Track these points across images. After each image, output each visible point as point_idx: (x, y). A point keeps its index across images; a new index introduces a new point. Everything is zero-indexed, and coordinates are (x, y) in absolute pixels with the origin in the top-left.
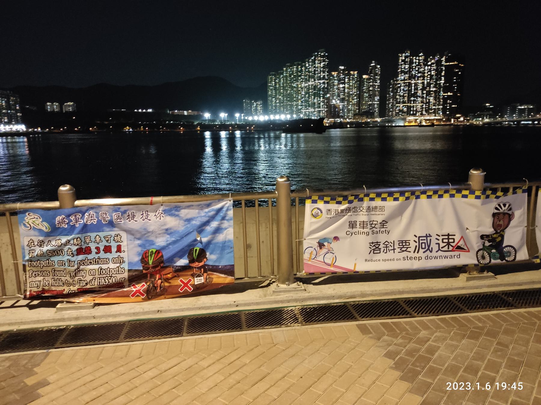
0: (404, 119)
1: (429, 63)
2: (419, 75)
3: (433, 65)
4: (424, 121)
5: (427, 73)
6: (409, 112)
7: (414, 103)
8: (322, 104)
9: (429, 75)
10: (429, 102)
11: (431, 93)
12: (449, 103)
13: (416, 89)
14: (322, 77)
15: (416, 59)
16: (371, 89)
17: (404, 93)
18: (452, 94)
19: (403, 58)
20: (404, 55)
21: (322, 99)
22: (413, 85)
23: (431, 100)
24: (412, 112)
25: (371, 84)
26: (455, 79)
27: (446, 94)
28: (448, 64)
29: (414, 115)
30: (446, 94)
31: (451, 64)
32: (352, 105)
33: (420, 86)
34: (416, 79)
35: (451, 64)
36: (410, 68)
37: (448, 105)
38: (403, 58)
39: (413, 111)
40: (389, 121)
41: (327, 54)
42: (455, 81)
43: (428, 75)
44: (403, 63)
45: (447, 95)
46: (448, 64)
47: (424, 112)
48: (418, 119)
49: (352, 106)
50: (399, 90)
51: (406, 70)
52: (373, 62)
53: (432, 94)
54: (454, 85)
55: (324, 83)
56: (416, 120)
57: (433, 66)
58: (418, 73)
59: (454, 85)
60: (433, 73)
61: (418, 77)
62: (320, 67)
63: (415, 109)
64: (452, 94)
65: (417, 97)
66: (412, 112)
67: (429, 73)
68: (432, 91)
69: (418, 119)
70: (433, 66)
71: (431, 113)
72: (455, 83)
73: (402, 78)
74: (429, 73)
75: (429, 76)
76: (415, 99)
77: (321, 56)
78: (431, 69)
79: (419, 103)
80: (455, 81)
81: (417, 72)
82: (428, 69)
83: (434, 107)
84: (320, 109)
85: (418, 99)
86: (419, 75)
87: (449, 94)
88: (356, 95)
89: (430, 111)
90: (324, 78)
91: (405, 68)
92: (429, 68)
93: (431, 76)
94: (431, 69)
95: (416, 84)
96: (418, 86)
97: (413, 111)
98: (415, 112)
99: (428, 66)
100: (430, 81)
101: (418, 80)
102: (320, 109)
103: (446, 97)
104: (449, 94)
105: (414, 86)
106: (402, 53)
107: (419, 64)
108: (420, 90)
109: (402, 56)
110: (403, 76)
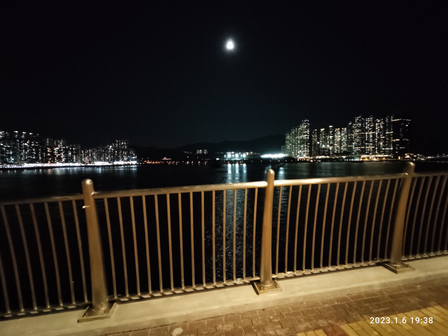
0: (359, 157)
1: (379, 121)
2: (370, 129)
3: (381, 122)
4: (375, 158)
5: (377, 127)
6: (363, 152)
7: (368, 146)
8: (305, 148)
9: (379, 128)
10: (380, 145)
11: (381, 140)
12: (398, 146)
13: (369, 138)
14: (305, 133)
15: (368, 119)
16: (349, 138)
17: (359, 141)
18: (399, 140)
19: (358, 120)
20: (358, 117)
21: (305, 146)
22: (367, 135)
23: (381, 145)
24: (367, 152)
25: (349, 135)
26: (401, 130)
27: (395, 140)
28: (395, 120)
29: (368, 154)
30: (395, 140)
31: (397, 120)
32: (343, 147)
33: (371, 136)
34: (368, 131)
35: (397, 120)
36: (362, 125)
37: (397, 147)
38: (358, 120)
39: (367, 151)
40: (351, 158)
41: (308, 121)
42: (401, 131)
43: (378, 129)
44: (358, 122)
45: (396, 141)
46: (395, 120)
47: (377, 152)
48: (370, 157)
49: (343, 148)
50: (356, 138)
51: (360, 127)
52: (351, 122)
53: (382, 140)
54: (400, 134)
55: (307, 137)
56: (369, 157)
57: (382, 123)
58: (369, 128)
59: (400, 134)
60: (382, 127)
61: (370, 130)
62: (305, 128)
63: (368, 150)
64: (399, 140)
65: (369, 142)
66: (367, 152)
67: (379, 127)
68: (382, 139)
69: (370, 157)
70: (382, 123)
71: (382, 153)
72: (401, 132)
73: (358, 131)
74: (379, 127)
75: (379, 129)
76: (368, 144)
77: (305, 122)
78: (380, 124)
79: (371, 146)
80: (401, 131)
81: (369, 127)
82: (378, 125)
83: (383, 149)
84: (304, 151)
85: (370, 144)
86: (370, 129)
87: (397, 140)
88: (345, 142)
89: (381, 152)
90: (307, 134)
91: (359, 126)
92: (379, 124)
93: (380, 129)
94: (380, 124)
95: (368, 135)
96: (370, 136)
97: (367, 151)
98: (368, 152)
99: (378, 123)
100: (380, 132)
101: (370, 132)
102: (304, 151)
103: (395, 142)
104: (397, 140)
105: (367, 136)
106: (357, 117)
107: (370, 122)
108: (371, 138)
109: (357, 119)
110: (358, 130)
